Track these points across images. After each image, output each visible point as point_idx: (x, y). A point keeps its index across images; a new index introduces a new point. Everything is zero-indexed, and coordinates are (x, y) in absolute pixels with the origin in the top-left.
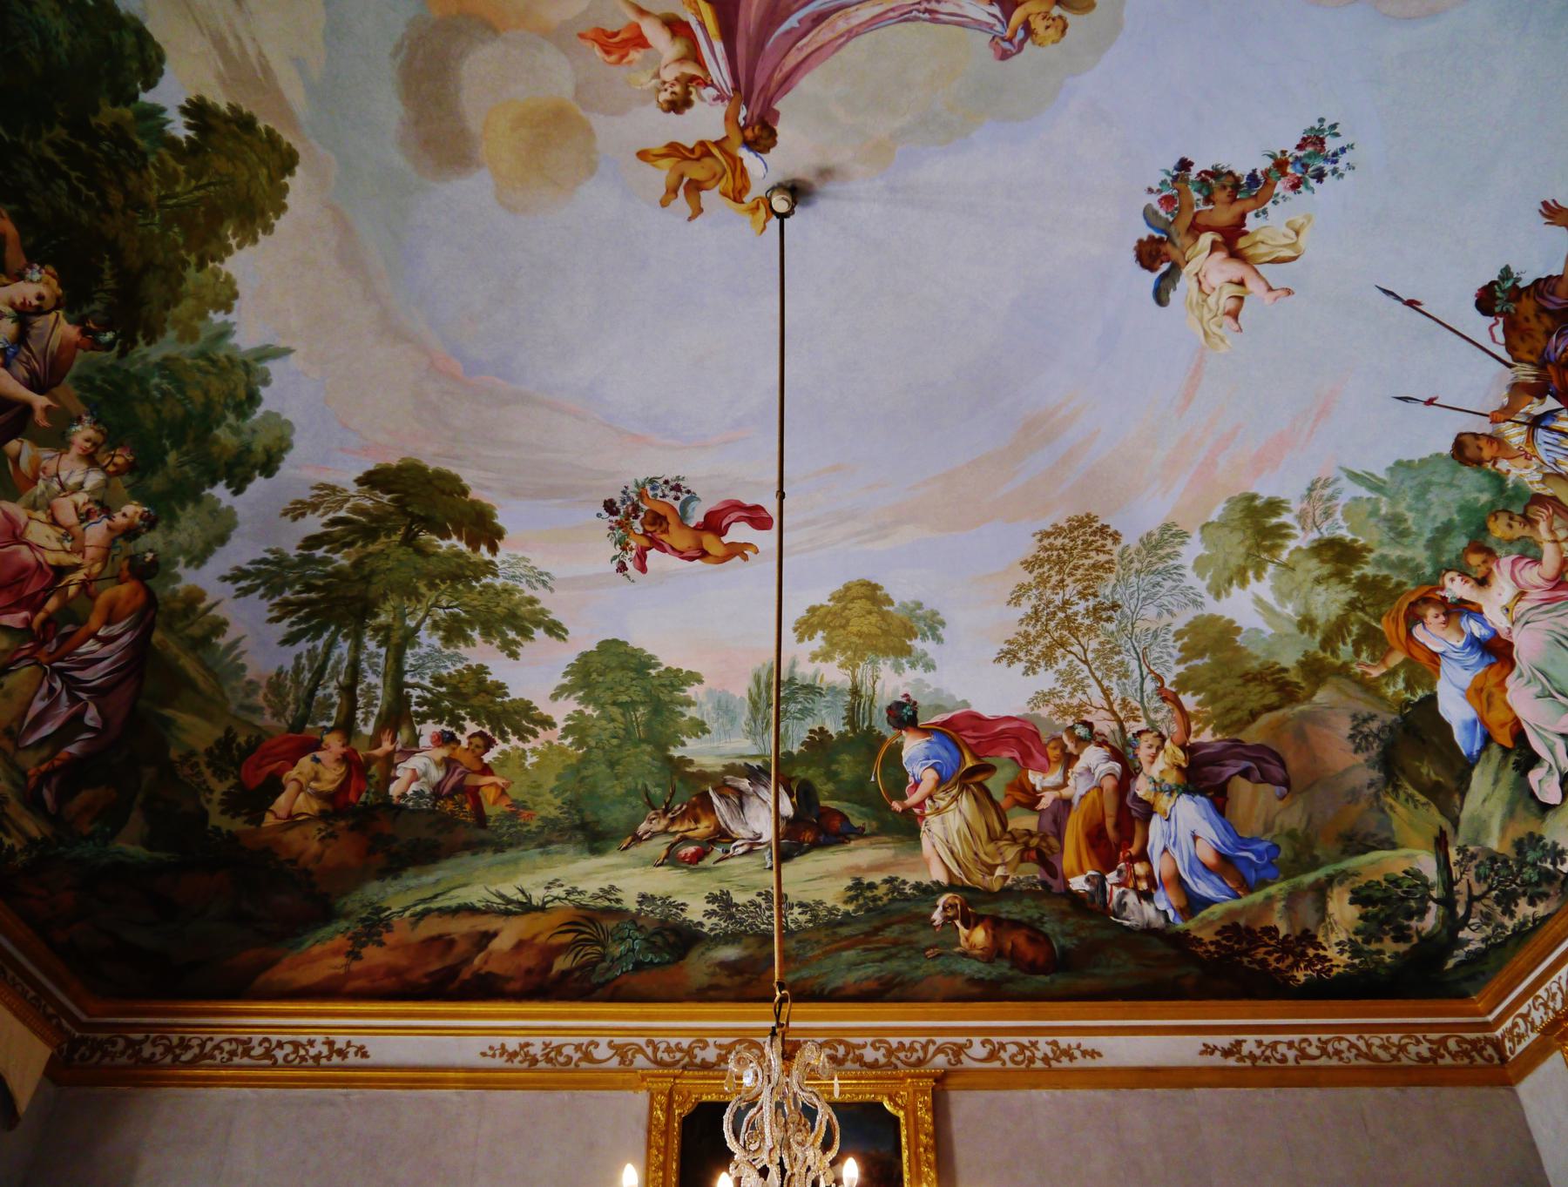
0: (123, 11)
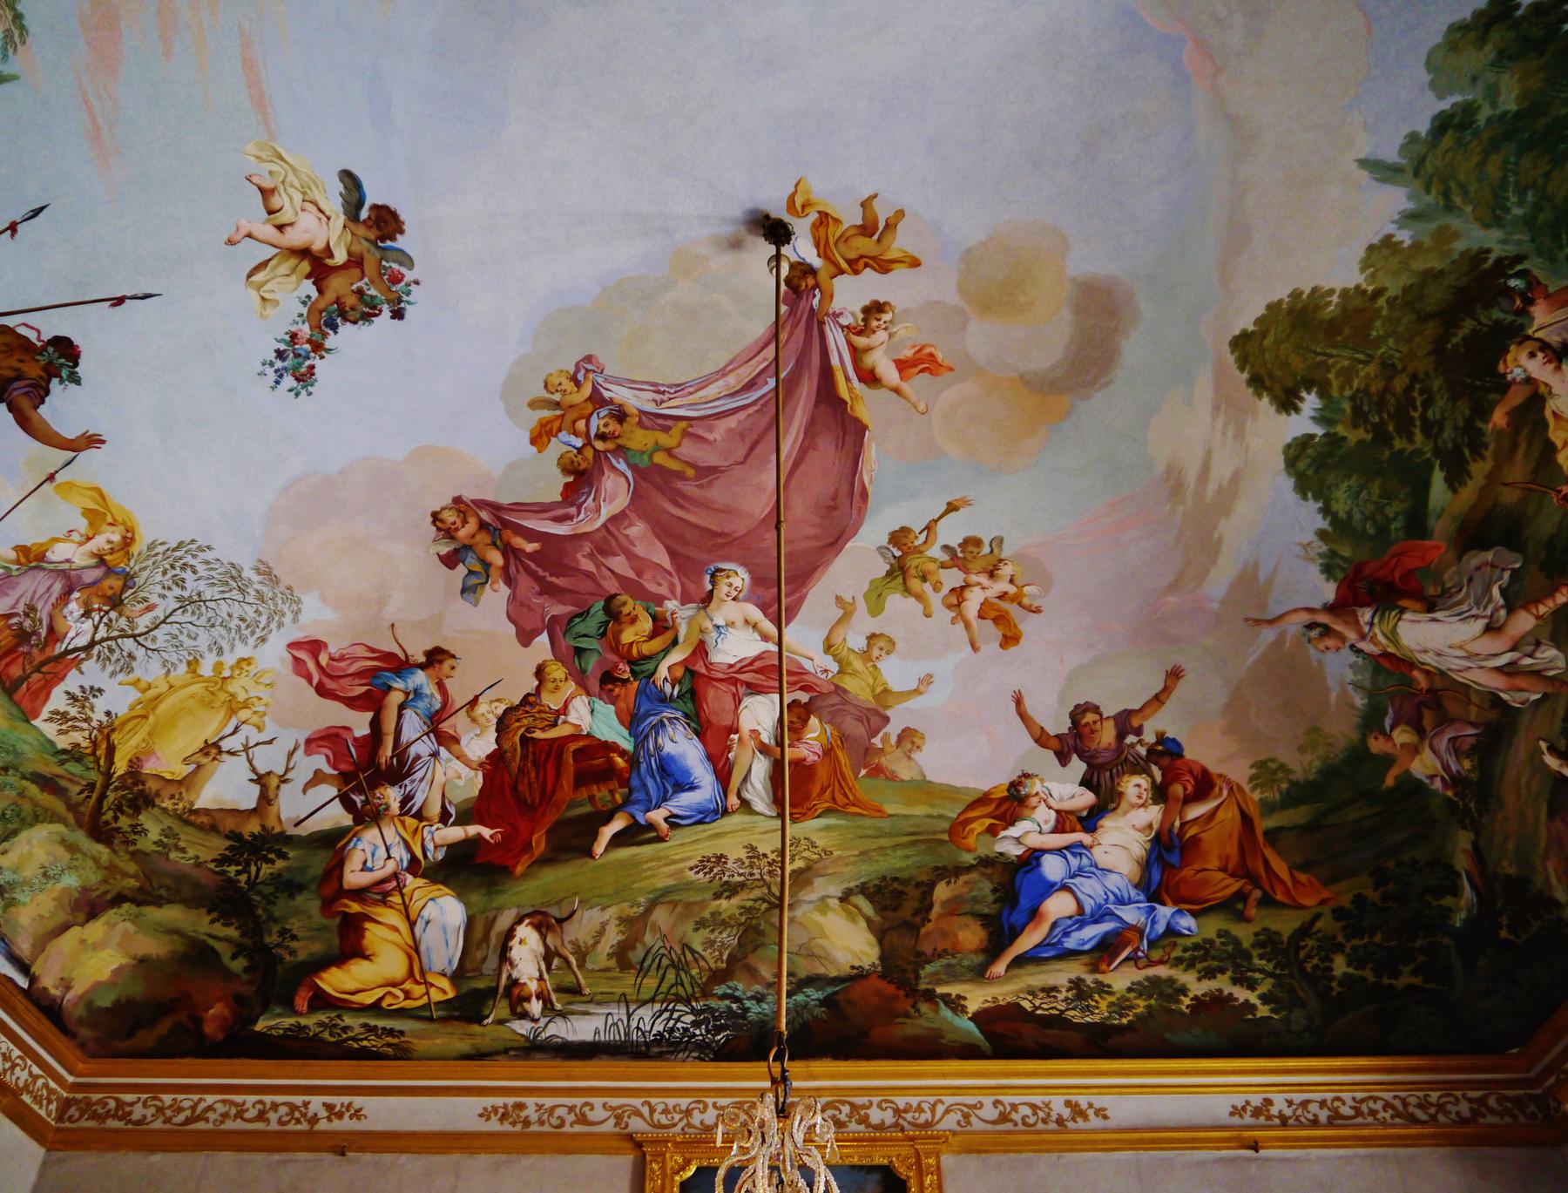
0: (1293, 480)
